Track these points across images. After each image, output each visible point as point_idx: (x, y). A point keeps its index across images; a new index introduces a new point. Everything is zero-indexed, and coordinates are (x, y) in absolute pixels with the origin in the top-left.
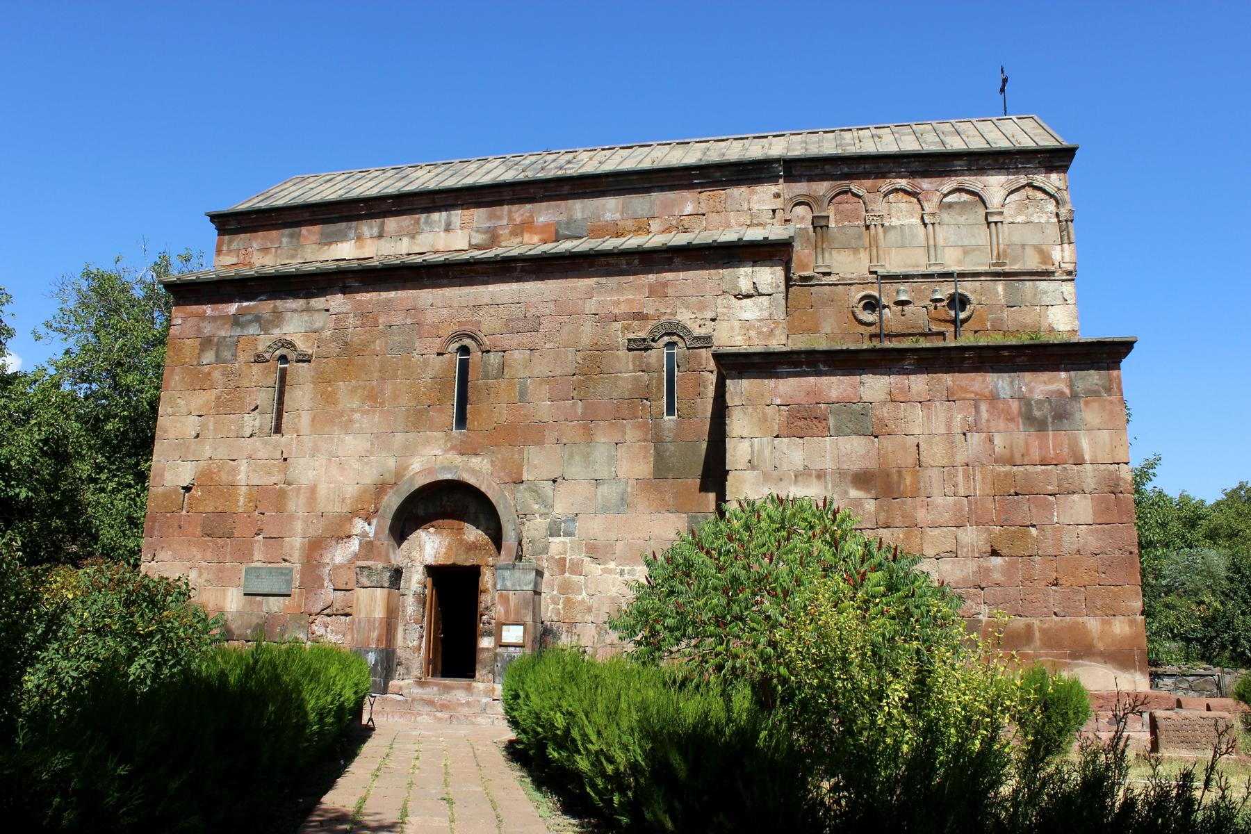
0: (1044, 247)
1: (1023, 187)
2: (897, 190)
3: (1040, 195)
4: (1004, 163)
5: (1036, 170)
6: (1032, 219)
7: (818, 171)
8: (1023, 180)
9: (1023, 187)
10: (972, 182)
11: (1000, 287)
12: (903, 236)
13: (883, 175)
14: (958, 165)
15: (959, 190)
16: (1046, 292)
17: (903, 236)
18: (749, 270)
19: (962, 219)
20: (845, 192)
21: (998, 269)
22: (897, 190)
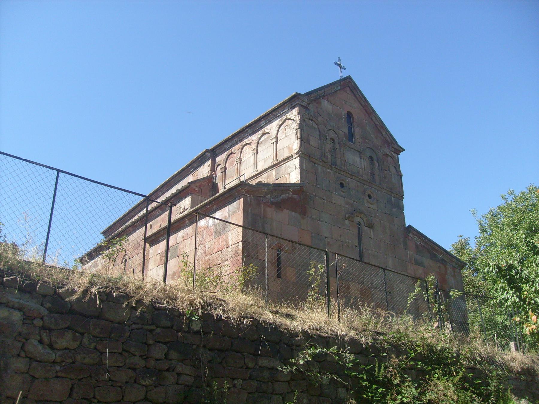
0: (290, 146)
1: (284, 121)
2: (246, 144)
3: (290, 122)
4: (277, 114)
5: (287, 112)
6: (287, 135)
7: (223, 149)
8: (283, 118)
9: (284, 121)
10: (267, 129)
11: (274, 172)
12: (246, 164)
13: (241, 141)
14: (262, 123)
15: (264, 134)
16: (289, 167)
17: (246, 164)
18: (183, 201)
19: (264, 147)
20: (232, 153)
21: (272, 164)
22: (246, 144)
